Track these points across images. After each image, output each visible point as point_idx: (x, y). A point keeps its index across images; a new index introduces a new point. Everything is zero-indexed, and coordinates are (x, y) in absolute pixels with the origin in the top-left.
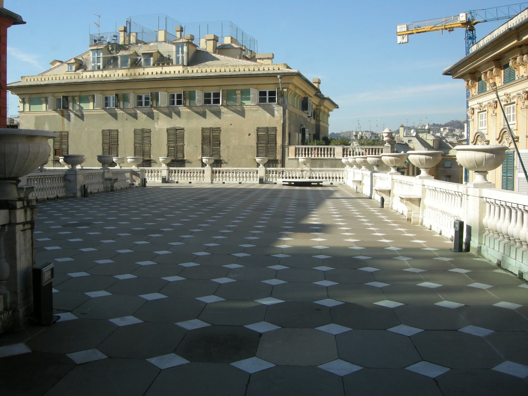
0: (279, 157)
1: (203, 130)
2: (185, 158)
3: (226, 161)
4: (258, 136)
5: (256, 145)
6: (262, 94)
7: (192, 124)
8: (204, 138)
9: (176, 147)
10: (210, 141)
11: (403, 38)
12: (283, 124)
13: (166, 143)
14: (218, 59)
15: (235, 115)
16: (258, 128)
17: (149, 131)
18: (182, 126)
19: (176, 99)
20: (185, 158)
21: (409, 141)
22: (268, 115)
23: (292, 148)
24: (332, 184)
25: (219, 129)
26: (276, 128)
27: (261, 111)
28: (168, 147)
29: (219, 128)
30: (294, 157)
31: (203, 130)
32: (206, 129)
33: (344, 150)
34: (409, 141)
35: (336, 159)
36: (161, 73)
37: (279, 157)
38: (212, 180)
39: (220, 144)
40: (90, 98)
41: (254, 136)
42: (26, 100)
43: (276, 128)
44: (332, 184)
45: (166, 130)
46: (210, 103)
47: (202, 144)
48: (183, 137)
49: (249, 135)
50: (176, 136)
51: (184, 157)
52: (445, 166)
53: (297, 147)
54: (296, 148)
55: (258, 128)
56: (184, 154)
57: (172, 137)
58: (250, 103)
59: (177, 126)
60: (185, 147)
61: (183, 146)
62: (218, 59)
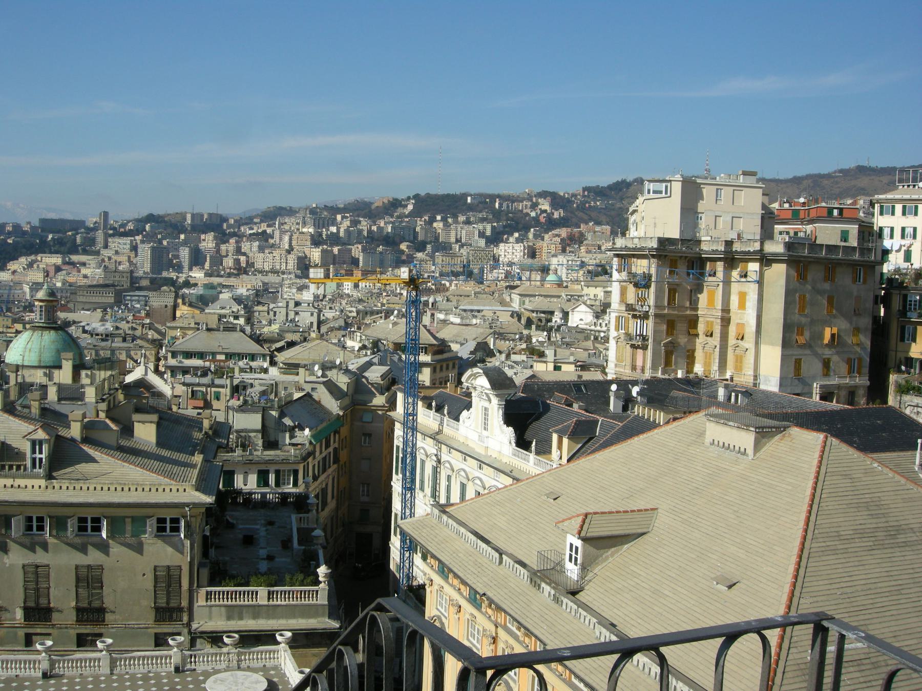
0: (185, 603)
1: (77, 567)
2: (52, 605)
3: (113, 609)
4: (156, 577)
5: (152, 588)
6: (161, 521)
7: (62, 560)
8: (78, 580)
9: (37, 590)
10: (88, 583)
11: (318, 288)
12: (190, 562)
13: (21, 584)
14: (94, 460)
15: (123, 549)
16: (155, 567)
18: (46, 562)
19: (35, 524)
20: (52, 605)
21: (313, 389)
22: (170, 550)
23: (203, 591)
24: (264, 666)
25: (101, 567)
26: (180, 566)
27: (160, 543)
28: (26, 589)
29: (101, 566)
30: (205, 604)
31: (77, 567)
32: (83, 566)
33: (269, 592)
34: (313, 389)
35: (260, 606)
36: (12, 486)
37: (185, 603)
38: (112, 670)
39: (102, 587)
41: (150, 576)
43: (180, 566)
44: (264, 666)
45: (21, 566)
46: (87, 531)
47: (77, 587)
49: (144, 575)
51: (49, 603)
52: (364, 420)
53: (209, 589)
54: (207, 592)
55: (155, 567)
56: (49, 600)
57: (31, 577)
58: (148, 538)
59: (39, 561)
60: (52, 590)
61: (48, 588)
62: (94, 460)
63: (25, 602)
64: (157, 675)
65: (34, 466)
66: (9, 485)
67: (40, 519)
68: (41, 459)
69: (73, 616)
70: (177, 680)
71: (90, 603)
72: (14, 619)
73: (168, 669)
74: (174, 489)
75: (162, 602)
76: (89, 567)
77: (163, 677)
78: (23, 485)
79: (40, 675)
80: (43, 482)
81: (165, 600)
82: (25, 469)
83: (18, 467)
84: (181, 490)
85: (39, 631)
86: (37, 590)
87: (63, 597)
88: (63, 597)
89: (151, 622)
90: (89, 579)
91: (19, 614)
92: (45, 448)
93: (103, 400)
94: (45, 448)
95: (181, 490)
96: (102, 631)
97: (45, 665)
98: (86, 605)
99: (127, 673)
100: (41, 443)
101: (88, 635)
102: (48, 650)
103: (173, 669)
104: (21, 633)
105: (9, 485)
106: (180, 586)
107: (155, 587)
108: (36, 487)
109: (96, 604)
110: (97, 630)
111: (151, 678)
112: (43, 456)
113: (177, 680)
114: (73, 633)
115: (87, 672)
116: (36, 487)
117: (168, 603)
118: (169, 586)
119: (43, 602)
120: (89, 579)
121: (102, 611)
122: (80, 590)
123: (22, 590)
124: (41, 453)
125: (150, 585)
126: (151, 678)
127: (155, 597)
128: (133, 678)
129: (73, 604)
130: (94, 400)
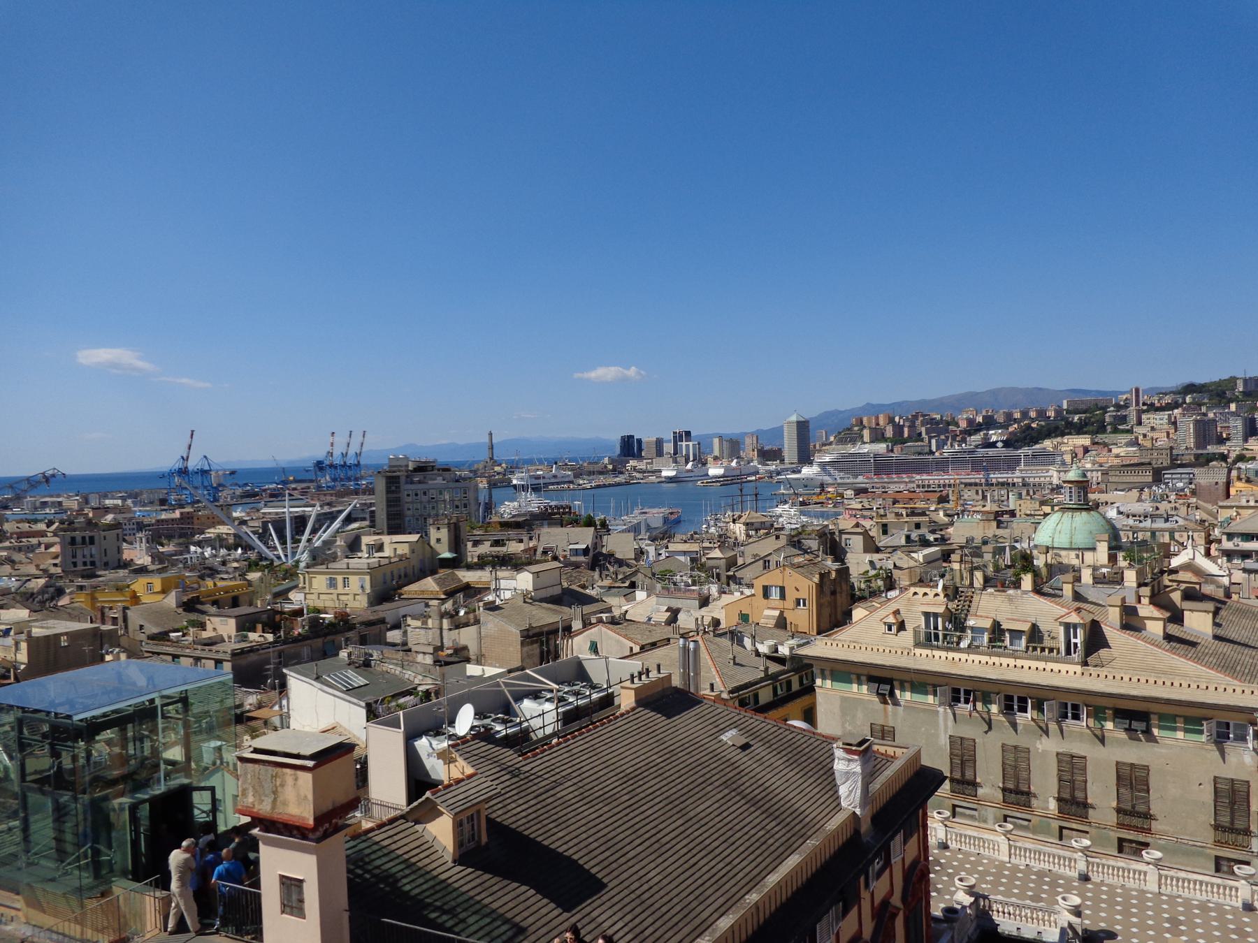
1: (1117, 763)
5: (1212, 803)
8: (1119, 777)
13: (1055, 772)
17: (1028, 751)
18: (1083, 754)
25: (1146, 768)
28: (1060, 780)
31: (1117, 763)
39: (1148, 791)
40: (930, 689)
42: (827, 673)
47: (1118, 785)
48: (1084, 769)
50: (1071, 768)
57: (1066, 767)
60: (1089, 785)
61: (1086, 782)
63: (1059, 792)
64: (1219, 907)
65: (1068, 652)
66: (1041, 668)
67: (1075, 707)
68: (1076, 644)
69: (1112, 818)
70: (1246, 920)
71: (1133, 807)
72: (1047, 809)
73: (1234, 903)
74: (1239, 690)
75: (1225, 820)
76: (1132, 765)
77: (1227, 912)
78: (1056, 670)
79: (1077, 875)
80: (1078, 668)
81: (1228, 819)
82: (1058, 652)
83: (1051, 650)
84: (1248, 692)
85: (1074, 826)
86: (1072, 782)
87: (1102, 795)
88: (1102, 795)
89: (1211, 841)
90: (1132, 780)
91: (1053, 805)
92: (1080, 632)
93: (1146, 585)
94: (1080, 632)
95: (1248, 692)
96: (1148, 840)
97: (1081, 865)
98: (1129, 808)
99: (1179, 896)
100: (1075, 626)
101: (1131, 841)
102: (1085, 850)
103: (1239, 904)
104: (1055, 825)
105: (1041, 668)
106: (1249, 806)
107: (1215, 801)
108: (1071, 673)
109: (1141, 808)
110: (1141, 837)
111: (1211, 909)
112: (1078, 641)
113: (1246, 920)
114: (1115, 835)
115: (1131, 884)
116: (1071, 673)
117: (1232, 822)
118: (1233, 803)
119: (1079, 795)
120: (1132, 780)
121: (1147, 816)
122: (1122, 790)
123: (1055, 780)
124: (1075, 637)
125: (1208, 795)
126: (1211, 909)
127: (1215, 814)
128: (1187, 903)
129: (1114, 804)
130: (1135, 585)
